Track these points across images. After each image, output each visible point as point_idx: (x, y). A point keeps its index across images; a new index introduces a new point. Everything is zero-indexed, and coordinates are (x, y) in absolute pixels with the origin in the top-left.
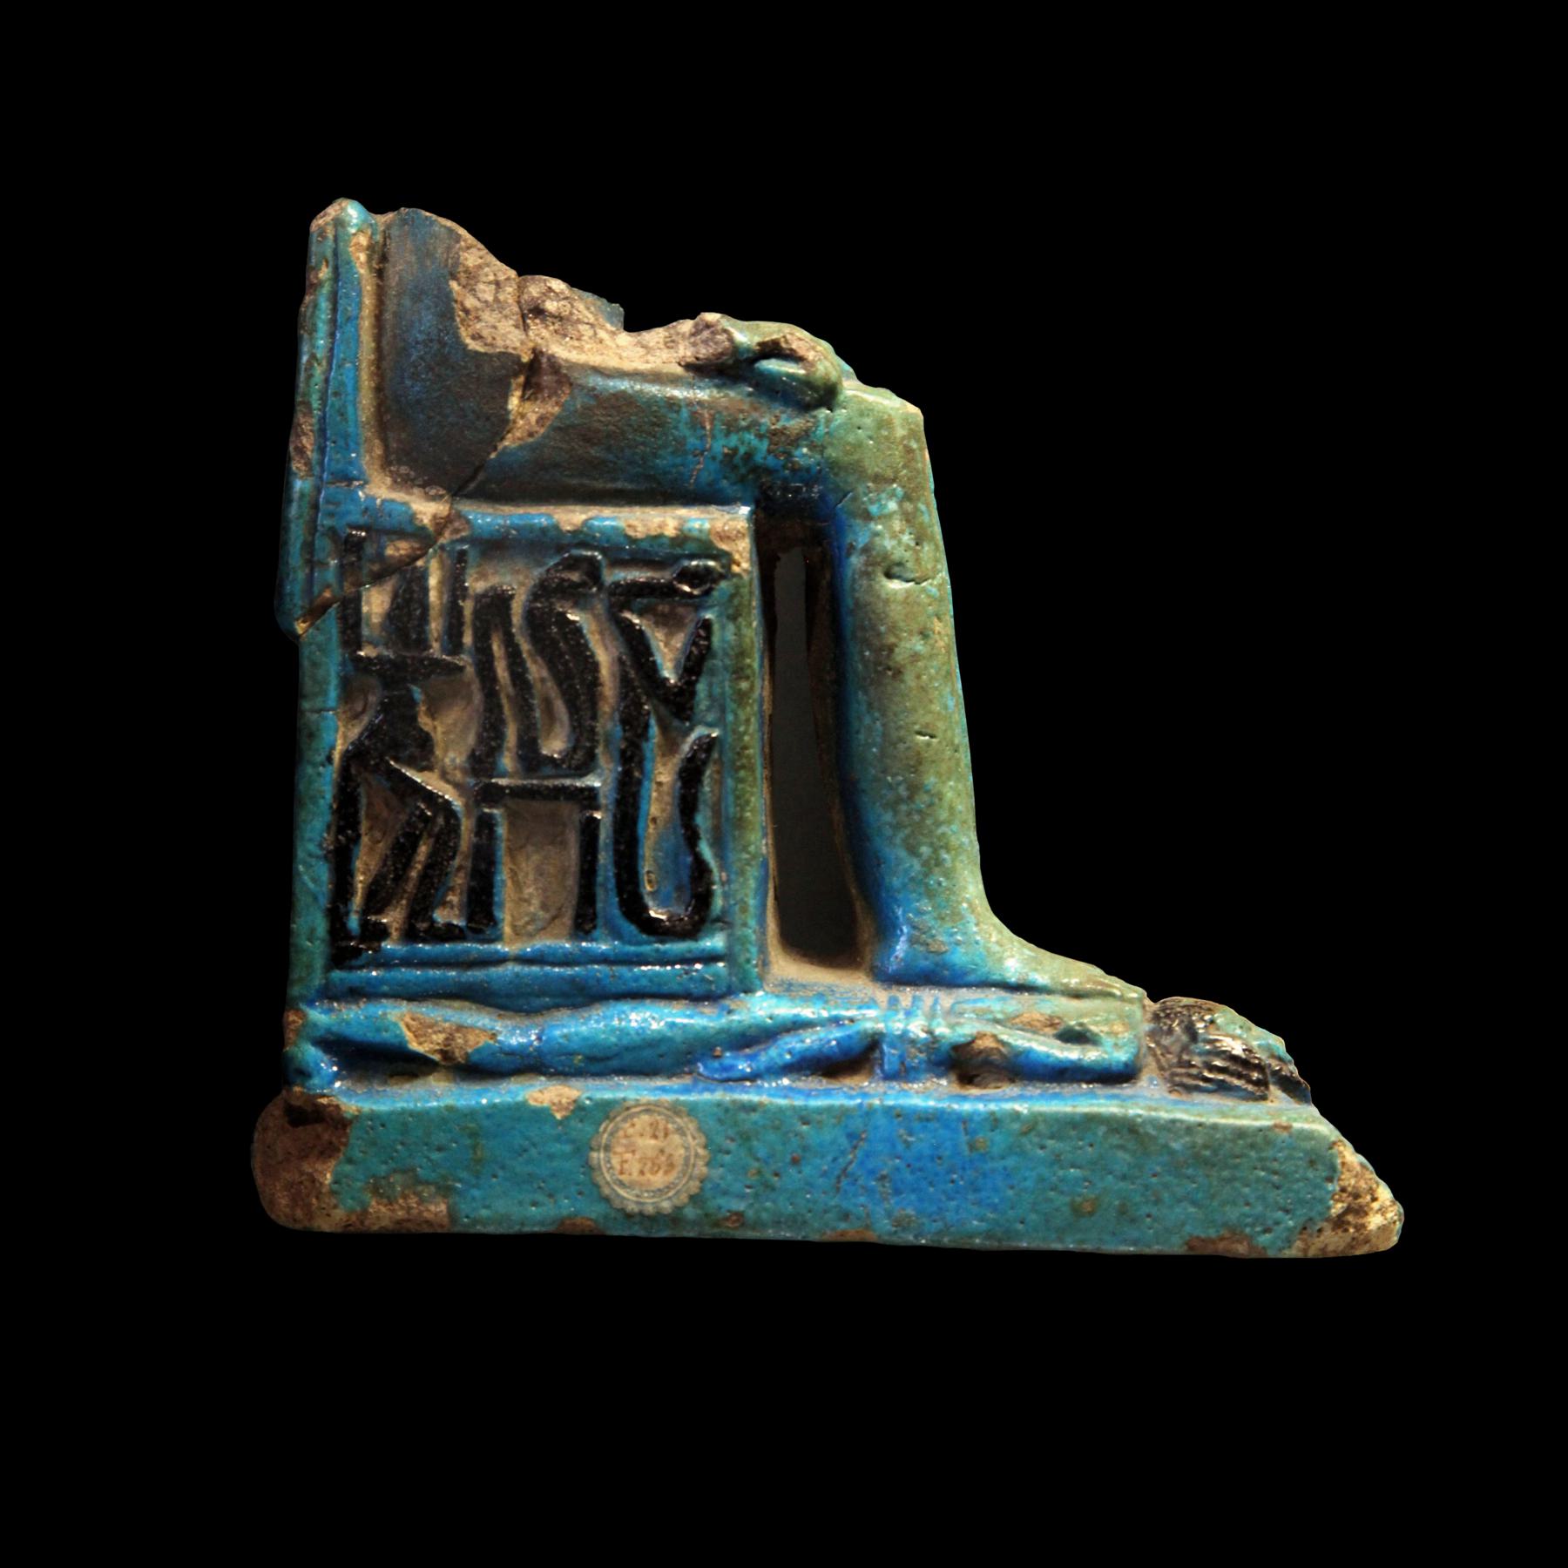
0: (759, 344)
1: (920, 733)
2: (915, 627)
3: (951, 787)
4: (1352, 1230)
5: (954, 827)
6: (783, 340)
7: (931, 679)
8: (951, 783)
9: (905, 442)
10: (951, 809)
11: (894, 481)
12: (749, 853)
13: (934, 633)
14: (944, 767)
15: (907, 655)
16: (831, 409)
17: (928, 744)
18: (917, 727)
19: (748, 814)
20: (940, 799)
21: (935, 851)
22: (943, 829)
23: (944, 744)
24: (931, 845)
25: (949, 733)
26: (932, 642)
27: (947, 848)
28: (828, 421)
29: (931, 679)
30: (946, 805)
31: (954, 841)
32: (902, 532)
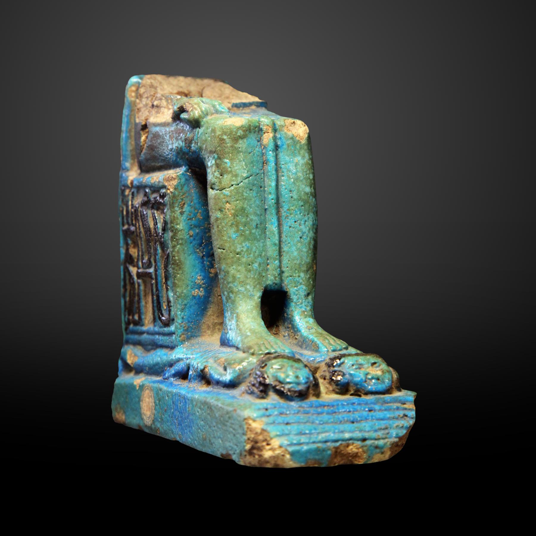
0: (178, 108)
1: (219, 248)
2: (217, 207)
3: (233, 268)
4: (257, 457)
5: (236, 284)
6: (184, 105)
7: (223, 227)
8: (234, 267)
9: (220, 137)
10: (234, 277)
11: (215, 152)
12: (176, 295)
13: (225, 209)
14: (229, 261)
15: (214, 219)
16: (200, 128)
17: (222, 252)
18: (218, 246)
19: (176, 281)
20: (228, 273)
21: (228, 294)
22: (231, 285)
23: (229, 251)
24: (227, 291)
25: (233, 248)
26: (224, 213)
27: (232, 292)
28: (198, 132)
29: (223, 227)
30: (230, 275)
31: (235, 289)
32: (215, 172)
